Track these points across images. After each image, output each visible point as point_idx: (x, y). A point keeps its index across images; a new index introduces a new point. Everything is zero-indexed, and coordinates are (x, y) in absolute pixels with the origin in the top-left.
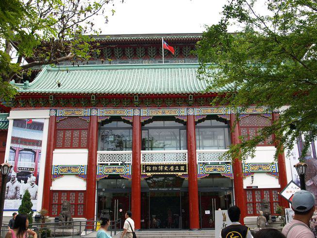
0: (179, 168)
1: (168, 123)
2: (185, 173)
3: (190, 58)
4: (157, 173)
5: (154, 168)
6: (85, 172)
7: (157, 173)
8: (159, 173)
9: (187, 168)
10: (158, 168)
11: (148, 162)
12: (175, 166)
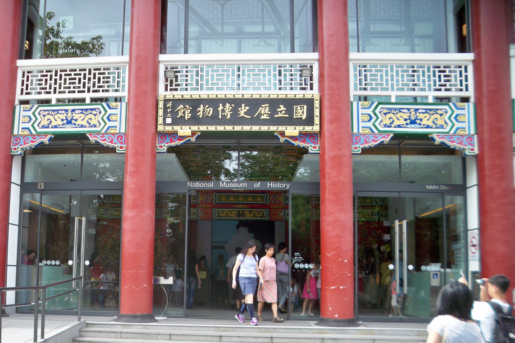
0: (290, 111)
2: (308, 129)
5: (201, 109)
7: (212, 128)
8: (220, 128)
9: (317, 112)
10: (216, 111)
11: (184, 93)
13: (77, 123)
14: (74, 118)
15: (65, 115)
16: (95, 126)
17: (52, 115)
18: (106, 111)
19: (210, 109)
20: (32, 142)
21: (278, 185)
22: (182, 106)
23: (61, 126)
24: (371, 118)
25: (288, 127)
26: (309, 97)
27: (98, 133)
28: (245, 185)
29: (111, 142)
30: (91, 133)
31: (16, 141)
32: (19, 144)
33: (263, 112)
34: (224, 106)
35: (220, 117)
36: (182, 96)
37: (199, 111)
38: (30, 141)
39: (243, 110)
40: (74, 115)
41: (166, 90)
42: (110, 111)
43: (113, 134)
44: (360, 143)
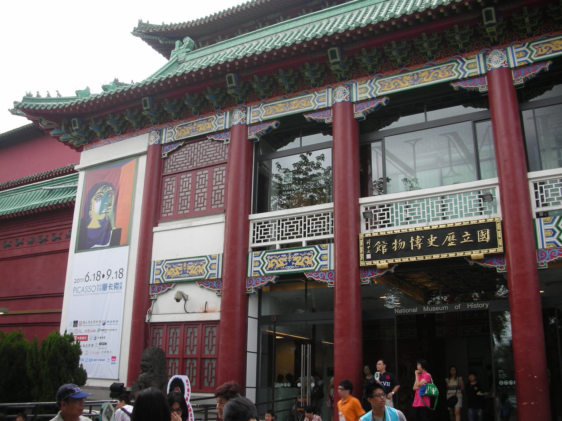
0: (474, 236)
2: (492, 251)
5: (395, 243)
6: (217, 272)
7: (405, 260)
8: (413, 259)
9: (499, 234)
10: (408, 244)
13: (296, 264)
14: (293, 260)
15: (287, 258)
16: (310, 266)
17: (276, 259)
18: (318, 252)
19: (403, 243)
20: (262, 282)
21: (477, 306)
22: (379, 242)
23: (283, 267)
24: (555, 232)
25: (474, 252)
26: (491, 220)
27: (313, 271)
28: (446, 308)
29: (323, 278)
30: (307, 271)
31: (250, 282)
32: (252, 285)
33: (449, 240)
34: (415, 238)
35: (412, 249)
36: (379, 233)
37: (394, 245)
38: (260, 281)
40: (293, 257)
41: (367, 228)
42: (321, 252)
43: (325, 272)
44: (546, 258)
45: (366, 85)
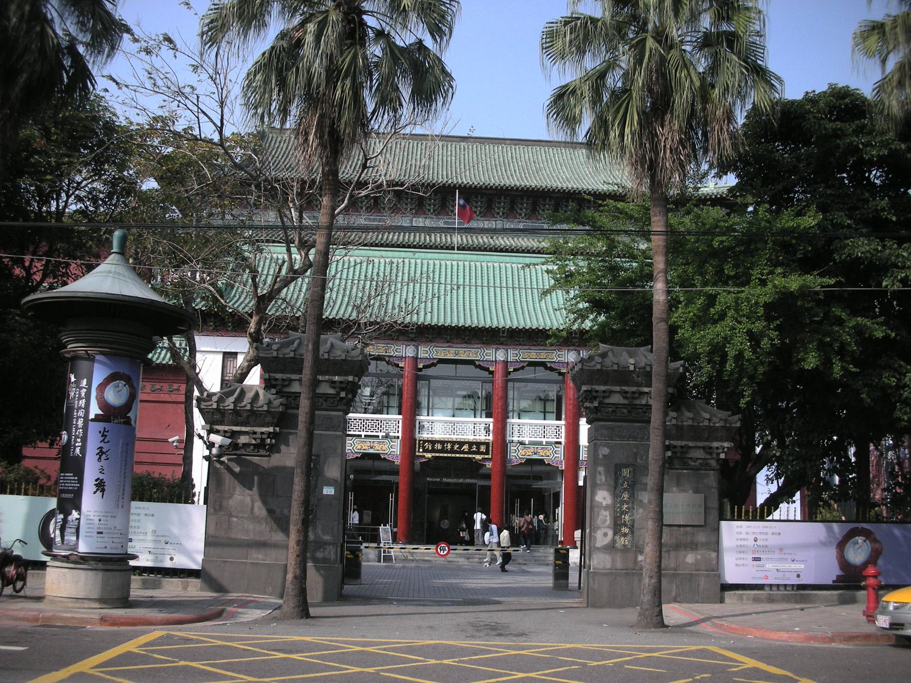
0: (478, 448)
1: (463, 370)
2: (486, 456)
3: (507, 218)
4: (441, 455)
7: (441, 455)
8: (445, 455)
12: (471, 444)
30: (382, 454)
39: (456, 446)
42: (392, 444)
45: (427, 349)
